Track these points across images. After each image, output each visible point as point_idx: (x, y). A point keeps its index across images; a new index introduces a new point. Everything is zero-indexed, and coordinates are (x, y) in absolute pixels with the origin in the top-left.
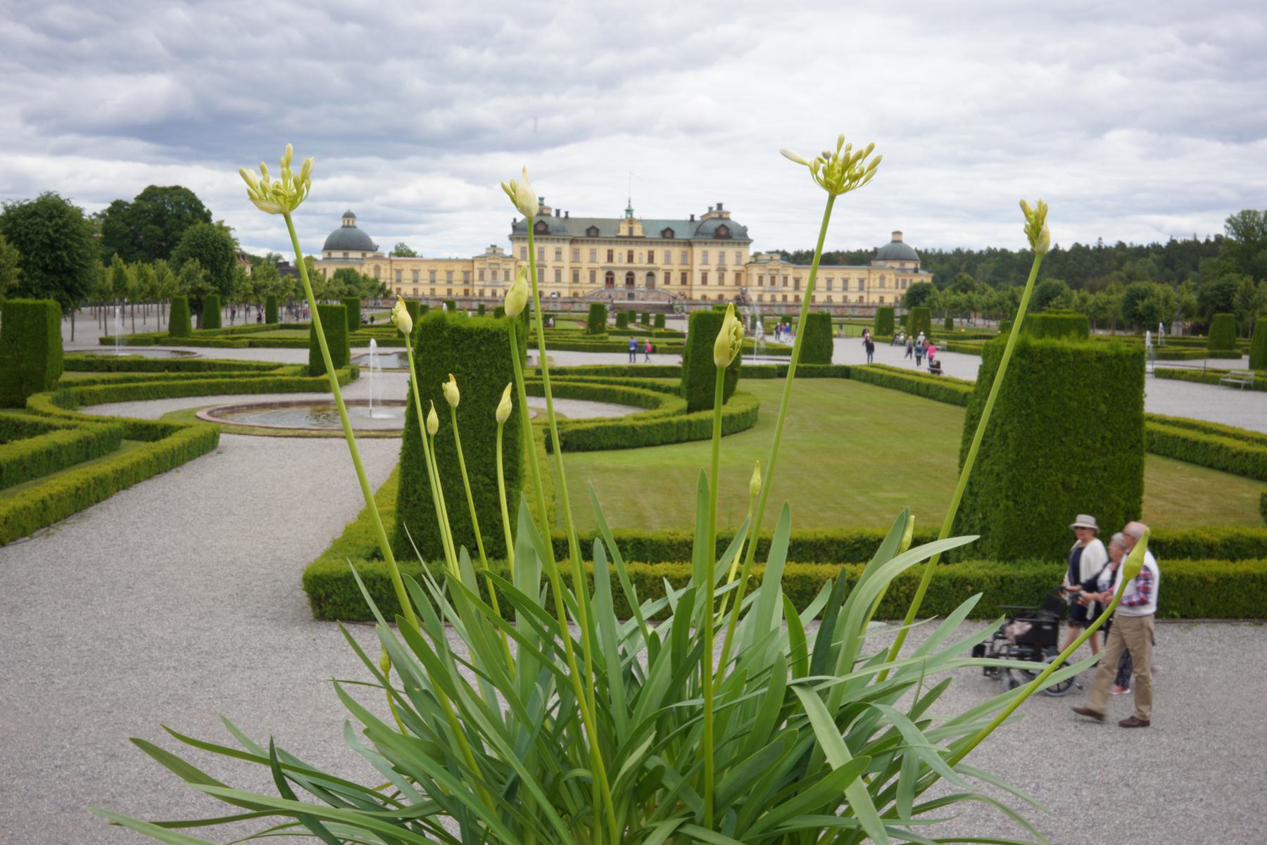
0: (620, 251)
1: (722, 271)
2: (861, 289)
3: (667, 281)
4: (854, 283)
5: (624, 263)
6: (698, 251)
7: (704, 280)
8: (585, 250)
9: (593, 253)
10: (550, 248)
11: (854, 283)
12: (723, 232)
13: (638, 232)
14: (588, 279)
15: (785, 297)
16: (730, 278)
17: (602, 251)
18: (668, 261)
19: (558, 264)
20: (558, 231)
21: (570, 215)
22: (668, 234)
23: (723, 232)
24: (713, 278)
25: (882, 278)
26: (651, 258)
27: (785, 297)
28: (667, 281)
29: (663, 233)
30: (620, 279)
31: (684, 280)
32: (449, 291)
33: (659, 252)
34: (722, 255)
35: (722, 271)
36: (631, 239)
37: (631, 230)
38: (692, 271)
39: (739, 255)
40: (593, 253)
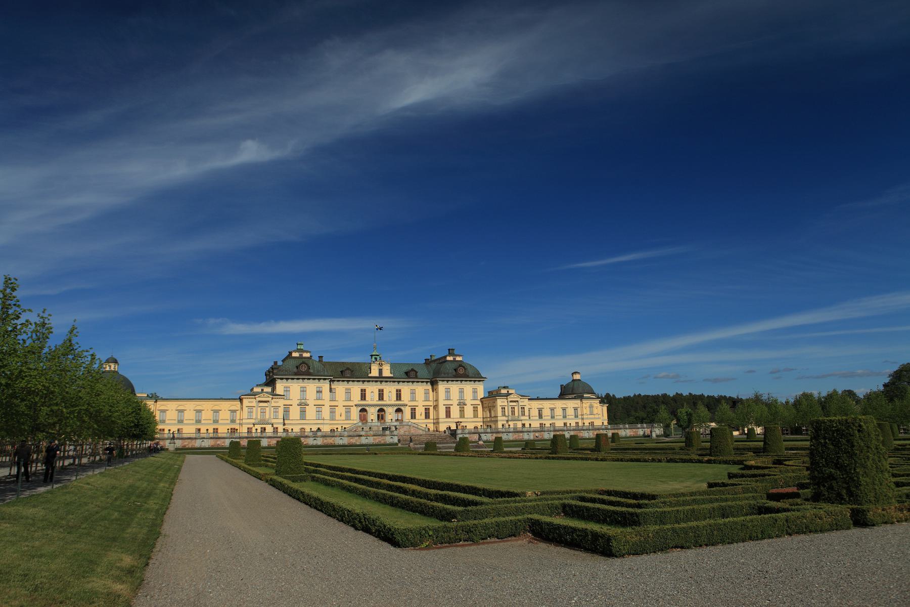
0: (372, 389)
1: (462, 405)
2: (576, 416)
3: (413, 416)
4: (570, 412)
5: (376, 400)
6: (442, 387)
7: (448, 414)
8: (340, 388)
9: (348, 392)
10: (311, 387)
11: (570, 412)
12: (461, 371)
13: (387, 372)
14: (343, 417)
15: (524, 425)
16: (469, 411)
17: (356, 389)
18: (413, 399)
19: (319, 402)
20: (318, 371)
21: (324, 360)
22: (412, 374)
23: (461, 371)
24: (455, 412)
25: (591, 407)
26: (399, 397)
27: (524, 425)
28: (413, 416)
29: (407, 373)
30: (372, 414)
31: (427, 416)
32: (216, 430)
33: (406, 389)
34: (461, 391)
35: (462, 405)
36: (380, 379)
37: (380, 371)
38: (436, 407)
39: (475, 392)
40: (348, 392)
